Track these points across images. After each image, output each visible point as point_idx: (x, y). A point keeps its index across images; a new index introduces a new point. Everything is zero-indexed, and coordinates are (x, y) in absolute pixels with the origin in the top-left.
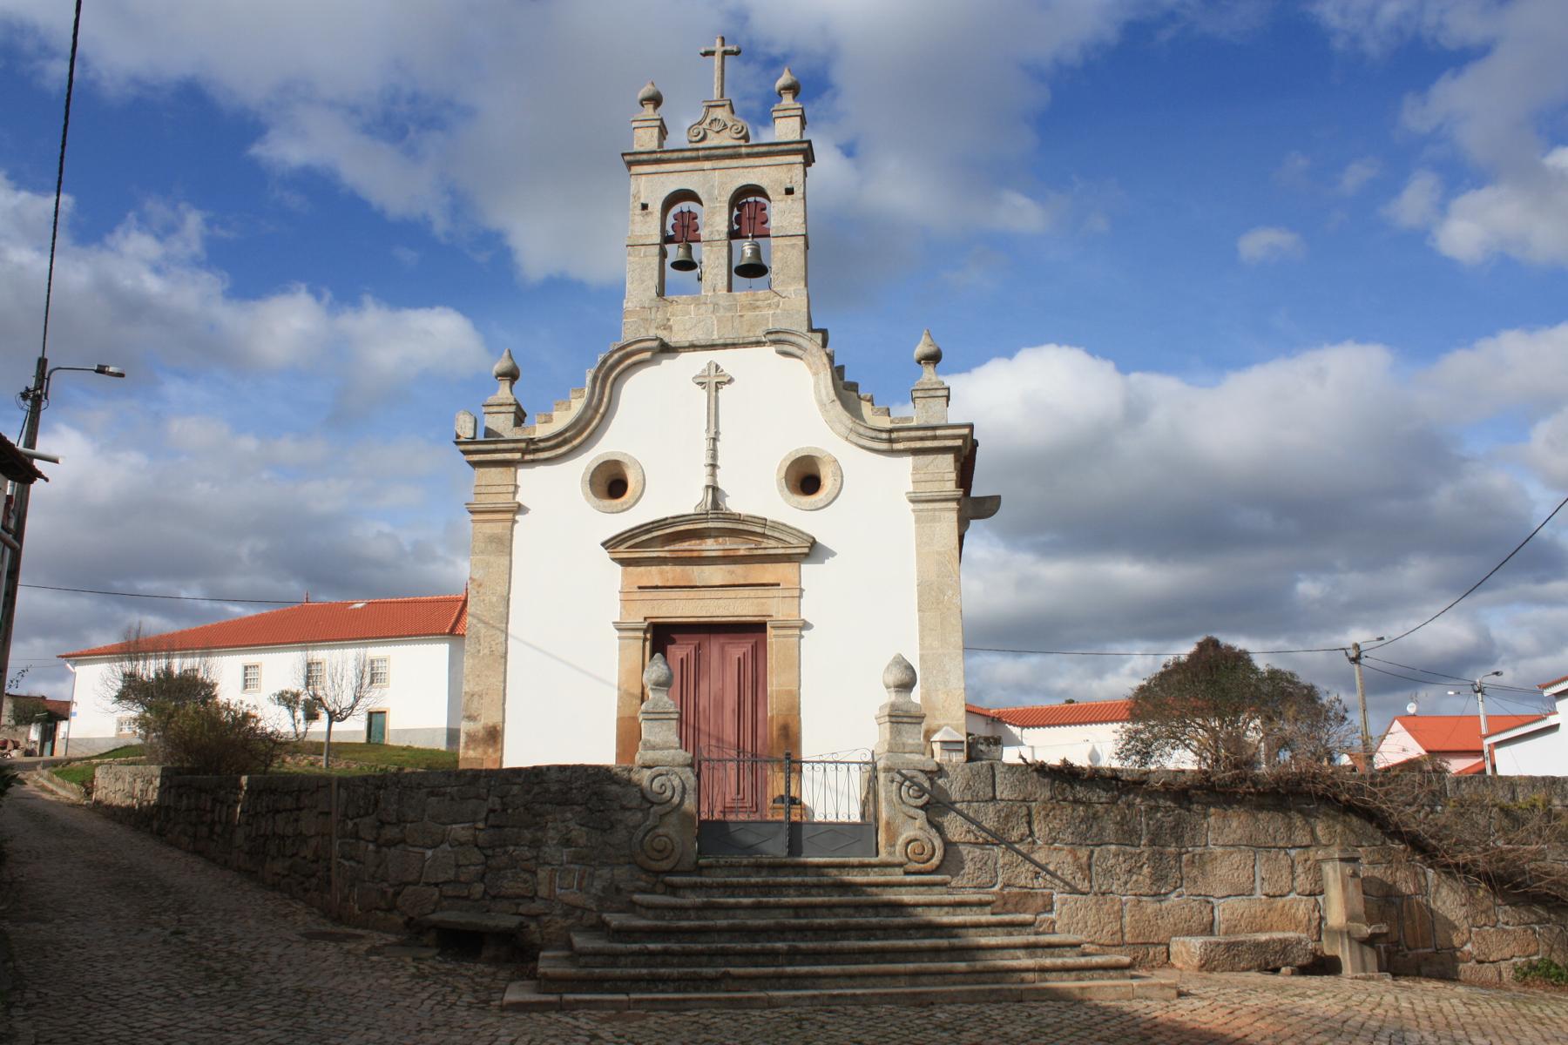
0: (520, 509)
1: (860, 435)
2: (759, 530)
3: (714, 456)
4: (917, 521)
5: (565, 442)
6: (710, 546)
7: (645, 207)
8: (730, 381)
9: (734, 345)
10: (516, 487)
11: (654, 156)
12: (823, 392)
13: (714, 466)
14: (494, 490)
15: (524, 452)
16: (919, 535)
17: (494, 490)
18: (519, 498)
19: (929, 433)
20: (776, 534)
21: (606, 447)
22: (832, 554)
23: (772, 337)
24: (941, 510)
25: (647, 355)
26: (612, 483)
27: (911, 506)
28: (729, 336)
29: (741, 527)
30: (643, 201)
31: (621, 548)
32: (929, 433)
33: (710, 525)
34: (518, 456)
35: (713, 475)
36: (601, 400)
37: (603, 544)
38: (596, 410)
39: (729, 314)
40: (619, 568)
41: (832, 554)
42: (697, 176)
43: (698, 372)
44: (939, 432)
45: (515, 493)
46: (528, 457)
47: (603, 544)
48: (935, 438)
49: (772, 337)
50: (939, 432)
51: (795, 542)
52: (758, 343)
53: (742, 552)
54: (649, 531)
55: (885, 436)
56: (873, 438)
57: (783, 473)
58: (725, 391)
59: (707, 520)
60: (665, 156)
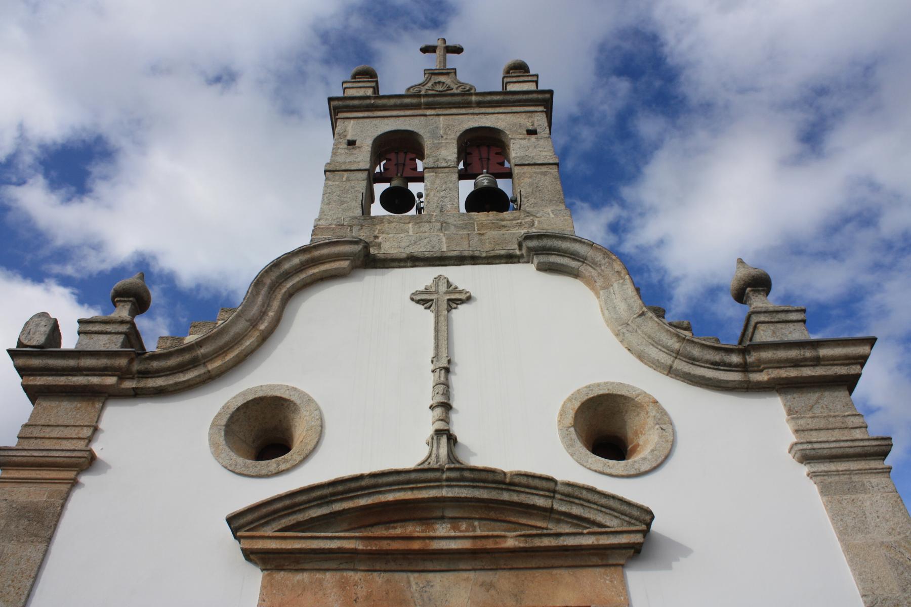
0: (89, 463)
1: (693, 360)
2: (540, 502)
3: (445, 387)
4: (825, 490)
5: (194, 363)
6: (445, 535)
7: (351, 143)
8: (469, 299)
9: (474, 260)
10: (96, 429)
11: (368, 102)
12: (622, 307)
13: (447, 406)
14: (56, 433)
15: (123, 374)
16: (837, 516)
17: (56, 433)
18: (96, 447)
19: (808, 353)
20: (576, 510)
21: (262, 377)
22: (683, 551)
23: (533, 244)
24: (861, 472)
25: (345, 264)
26: (265, 432)
27: (805, 469)
28: (463, 248)
29: (506, 496)
30: (349, 137)
31: (268, 531)
32: (808, 353)
33: (445, 492)
34: (111, 380)
35: (446, 420)
36: (263, 314)
37: (230, 520)
38: (254, 323)
39: (466, 232)
40: (255, 576)
41: (683, 551)
42: (416, 120)
43: (421, 288)
44: (824, 352)
45: (90, 440)
46: (129, 384)
47: (230, 520)
48: (817, 361)
49: (533, 244)
50: (824, 352)
51: (613, 523)
52: (510, 259)
53: (510, 543)
54: (324, 501)
55: (735, 359)
56: (715, 365)
57: (569, 419)
58: (460, 314)
59: (437, 483)
60: (380, 102)
